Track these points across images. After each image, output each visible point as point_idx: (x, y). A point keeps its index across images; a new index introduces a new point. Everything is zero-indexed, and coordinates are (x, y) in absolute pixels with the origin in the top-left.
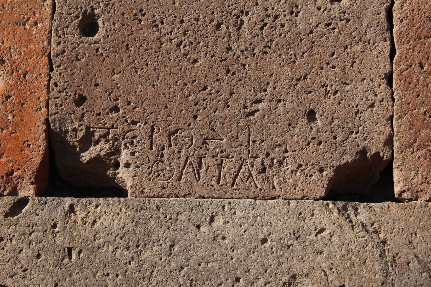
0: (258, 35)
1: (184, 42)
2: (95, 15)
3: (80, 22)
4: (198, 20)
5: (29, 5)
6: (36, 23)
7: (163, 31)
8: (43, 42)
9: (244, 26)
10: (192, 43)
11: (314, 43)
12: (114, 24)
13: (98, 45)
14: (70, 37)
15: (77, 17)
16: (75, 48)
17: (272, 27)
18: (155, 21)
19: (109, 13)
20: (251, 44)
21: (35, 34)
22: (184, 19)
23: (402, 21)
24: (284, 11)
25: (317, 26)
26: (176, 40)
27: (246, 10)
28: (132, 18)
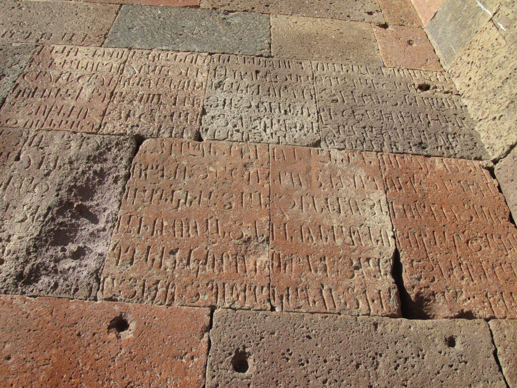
0: (394, 375)
1: (329, 380)
2: (246, 353)
3: (234, 358)
4: (339, 361)
5: (187, 341)
6: (192, 358)
7: (309, 370)
8: (198, 375)
9: (380, 366)
10: (336, 381)
11: (442, 382)
12: (264, 361)
13: (249, 380)
14: (223, 372)
15: (230, 354)
16: (228, 382)
17: (404, 368)
18: (301, 360)
19: (259, 351)
20: (389, 383)
21: (191, 367)
22: (327, 359)
23: (508, 363)
24: (412, 354)
25: (442, 367)
26: (321, 377)
27: (380, 353)
28: (281, 357)
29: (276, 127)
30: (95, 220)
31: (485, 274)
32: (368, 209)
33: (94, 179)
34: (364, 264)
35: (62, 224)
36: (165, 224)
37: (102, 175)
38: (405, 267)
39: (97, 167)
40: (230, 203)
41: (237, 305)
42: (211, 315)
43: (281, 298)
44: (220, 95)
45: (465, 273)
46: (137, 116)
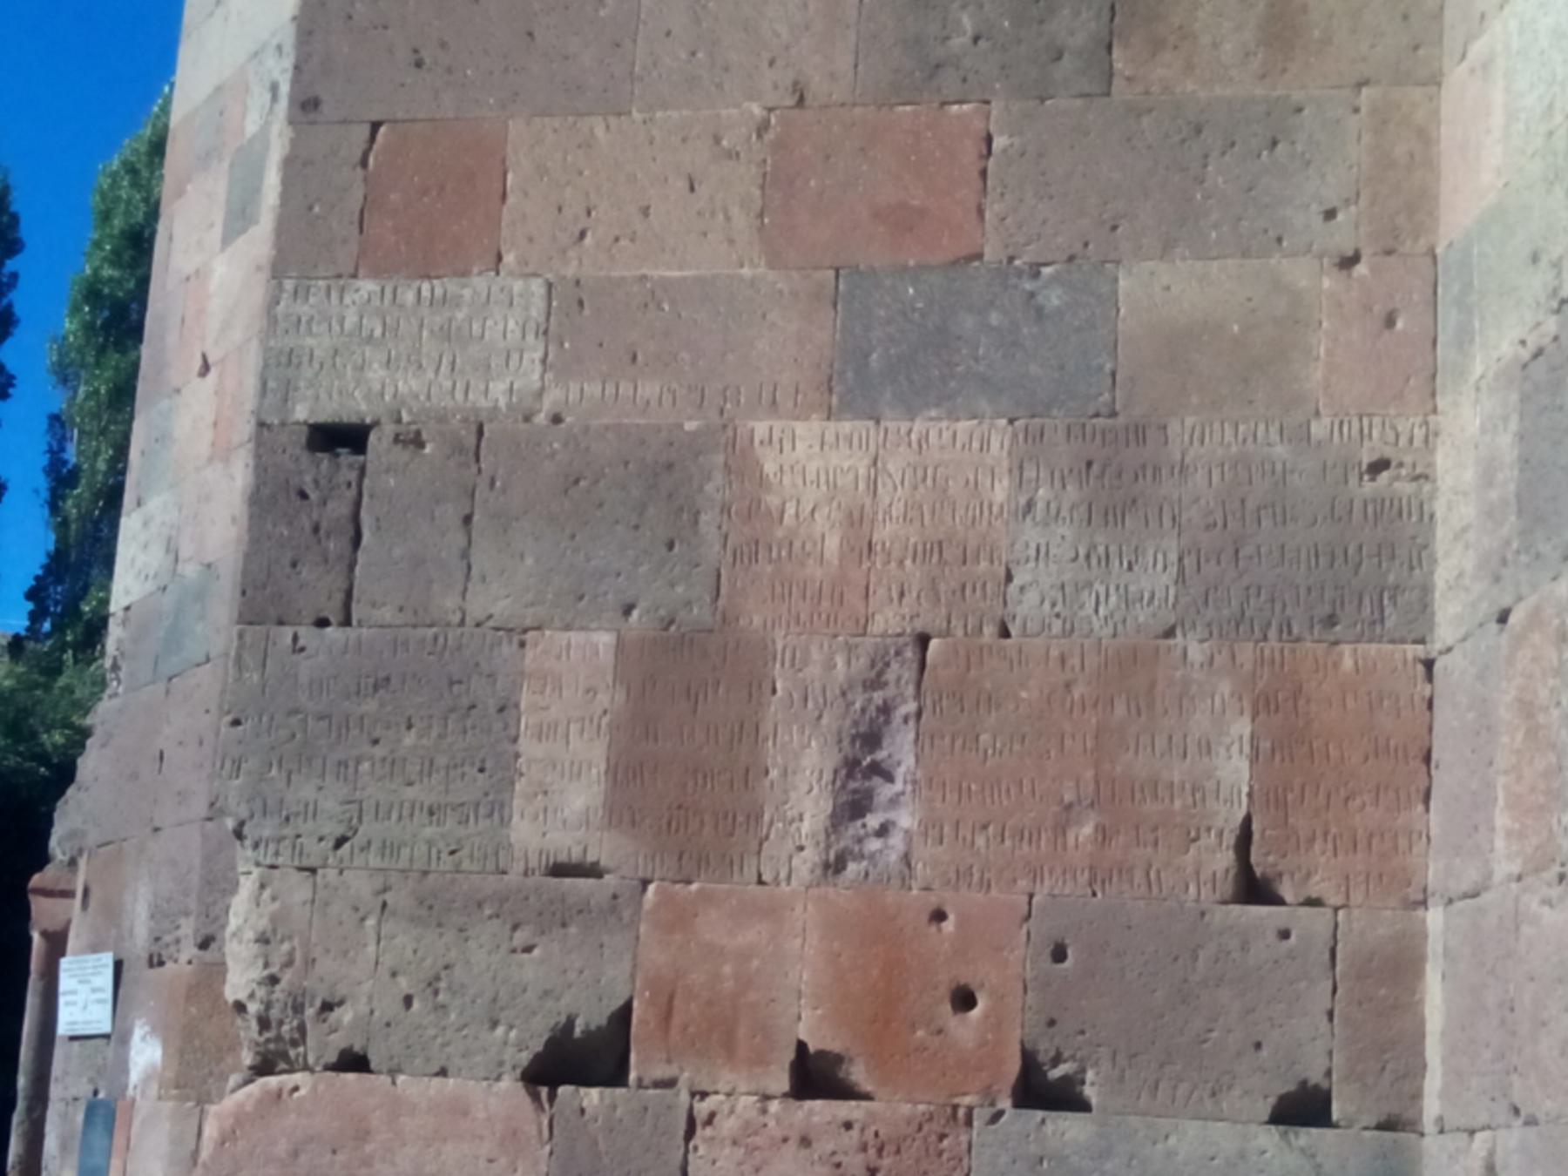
29: (1113, 599)
30: (889, 778)
31: (1355, 846)
32: (1222, 751)
33: (878, 717)
34: (1203, 834)
35: (855, 791)
36: (973, 787)
37: (886, 710)
38: (1256, 837)
39: (878, 697)
40: (1048, 752)
41: (1056, 891)
42: (1030, 903)
43: (1103, 882)
44: (1031, 534)
45: (1330, 846)
46: (914, 594)
